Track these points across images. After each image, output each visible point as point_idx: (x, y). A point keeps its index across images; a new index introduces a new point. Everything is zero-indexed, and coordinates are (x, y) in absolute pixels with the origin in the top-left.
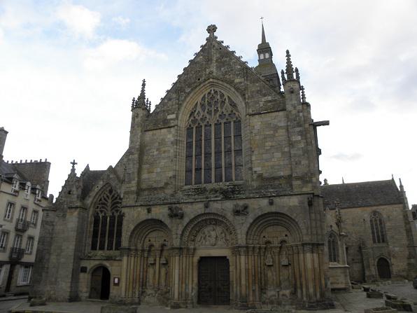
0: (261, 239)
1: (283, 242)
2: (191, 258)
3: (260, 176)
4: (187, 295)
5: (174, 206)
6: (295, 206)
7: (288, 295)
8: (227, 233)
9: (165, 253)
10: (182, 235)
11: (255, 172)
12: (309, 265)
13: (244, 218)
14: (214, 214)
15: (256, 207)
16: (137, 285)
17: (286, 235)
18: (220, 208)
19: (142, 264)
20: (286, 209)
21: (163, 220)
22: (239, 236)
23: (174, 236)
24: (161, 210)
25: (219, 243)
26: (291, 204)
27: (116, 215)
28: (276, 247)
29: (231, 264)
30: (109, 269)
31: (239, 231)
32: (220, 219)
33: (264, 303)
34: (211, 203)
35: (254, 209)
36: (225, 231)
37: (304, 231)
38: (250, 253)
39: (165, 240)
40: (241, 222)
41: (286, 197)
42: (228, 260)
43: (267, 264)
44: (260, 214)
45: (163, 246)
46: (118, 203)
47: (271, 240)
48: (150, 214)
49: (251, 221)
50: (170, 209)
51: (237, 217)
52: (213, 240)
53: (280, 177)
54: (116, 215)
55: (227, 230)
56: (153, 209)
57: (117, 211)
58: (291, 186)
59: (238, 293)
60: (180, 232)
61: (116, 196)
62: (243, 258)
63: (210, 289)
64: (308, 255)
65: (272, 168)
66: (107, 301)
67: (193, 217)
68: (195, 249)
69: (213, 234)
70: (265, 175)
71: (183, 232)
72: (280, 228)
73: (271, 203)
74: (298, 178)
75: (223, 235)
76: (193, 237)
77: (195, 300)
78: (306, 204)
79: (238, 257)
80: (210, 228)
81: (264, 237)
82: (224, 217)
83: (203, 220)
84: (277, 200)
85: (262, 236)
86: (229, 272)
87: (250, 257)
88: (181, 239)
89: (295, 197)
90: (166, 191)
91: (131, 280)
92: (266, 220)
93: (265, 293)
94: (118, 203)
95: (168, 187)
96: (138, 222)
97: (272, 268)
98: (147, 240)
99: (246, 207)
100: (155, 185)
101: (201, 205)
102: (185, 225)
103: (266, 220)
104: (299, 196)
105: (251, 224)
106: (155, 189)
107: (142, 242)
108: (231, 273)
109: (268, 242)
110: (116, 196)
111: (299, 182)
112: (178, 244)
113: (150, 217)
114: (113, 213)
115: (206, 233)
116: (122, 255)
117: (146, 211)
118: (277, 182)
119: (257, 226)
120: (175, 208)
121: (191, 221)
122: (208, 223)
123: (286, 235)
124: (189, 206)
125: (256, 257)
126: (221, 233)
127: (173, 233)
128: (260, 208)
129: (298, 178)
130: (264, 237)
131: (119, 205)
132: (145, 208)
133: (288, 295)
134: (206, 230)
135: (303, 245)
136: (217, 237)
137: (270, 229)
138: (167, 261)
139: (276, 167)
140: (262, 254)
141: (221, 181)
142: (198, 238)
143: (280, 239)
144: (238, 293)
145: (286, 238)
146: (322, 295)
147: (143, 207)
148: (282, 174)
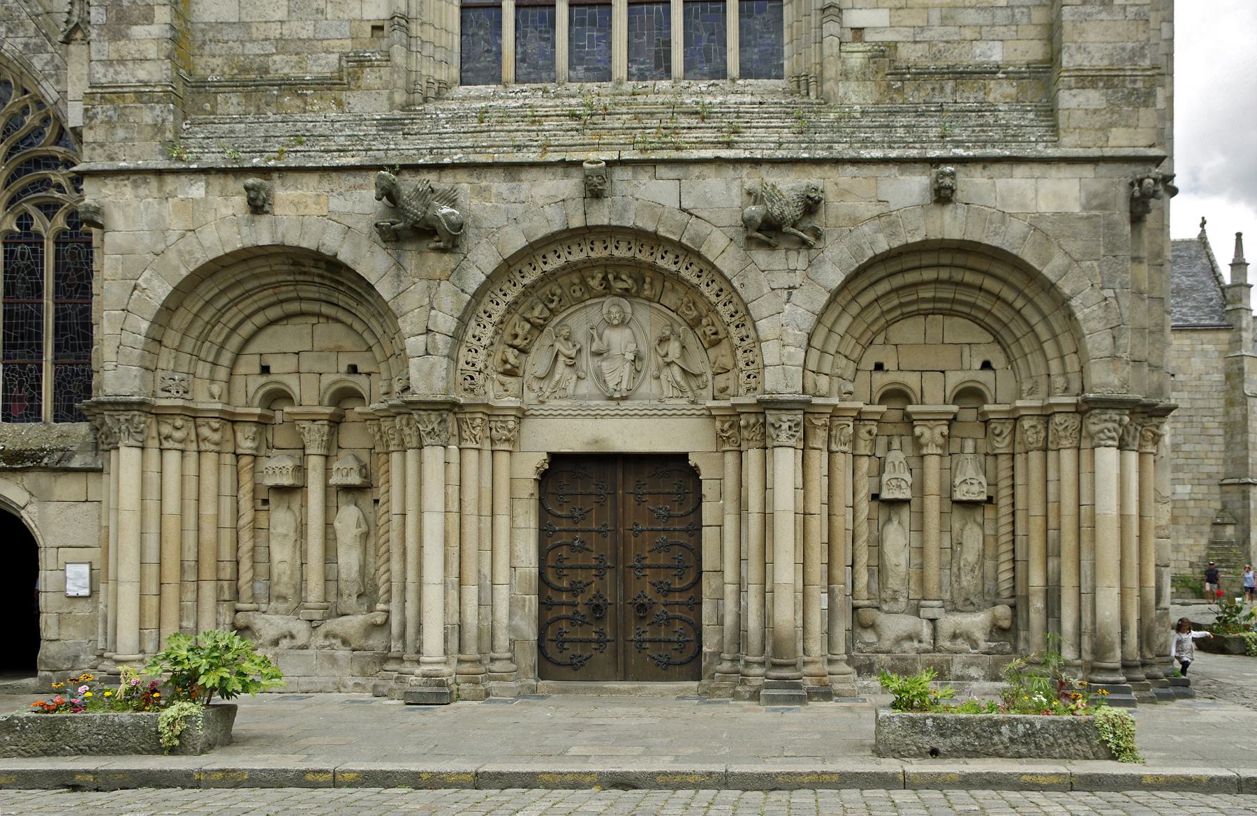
0: (863, 377)
1: (969, 394)
2: (503, 459)
3: (883, 54)
4: (488, 636)
5: (408, 184)
6: (1063, 218)
7: (980, 635)
8: (691, 339)
9: (352, 437)
10: (457, 338)
11: (858, 32)
12: (1108, 504)
13: (798, 260)
14: (638, 235)
15: (866, 209)
16: (208, 590)
17: (986, 365)
18: (672, 203)
19: (227, 488)
20: (1018, 227)
21: (344, 256)
22: (770, 352)
23: (415, 344)
24: (336, 203)
25: (648, 387)
26: (1045, 206)
27: (48, 228)
28: (931, 419)
29: (708, 488)
30: (29, 517)
31: (766, 327)
32: (667, 263)
33: (865, 669)
34: (620, 174)
35: (855, 221)
36: (682, 329)
37: (1097, 342)
38: (819, 439)
39: (353, 369)
40: (783, 280)
41: (1021, 170)
42: (694, 472)
43: (886, 495)
44: (883, 246)
45: (344, 396)
46: (50, 162)
47: (912, 380)
48: (264, 220)
49: (834, 277)
50: (389, 194)
51: (761, 256)
52: (618, 374)
53: (987, 72)
54: (48, 228)
55: (694, 324)
56: (284, 194)
57: (49, 209)
58: (1050, 112)
59: (753, 622)
60: (445, 322)
61: (30, 120)
62: (786, 462)
63: (597, 609)
64: (1108, 457)
65: (944, 21)
66: (30, 682)
67: (520, 242)
68: (522, 415)
69: (618, 339)
70: (909, 54)
71: (463, 322)
72: (959, 330)
73: (943, 196)
74: (1086, 80)
75: (674, 348)
76: (511, 355)
77: (529, 658)
78: (1121, 214)
79: (753, 457)
80: (611, 307)
81: (879, 367)
82: (689, 253)
83: (569, 268)
84: (972, 183)
85: (868, 363)
86: (696, 529)
87: (814, 455)
88: (452, 358)
89: (1067, 171)
90: (358, 102)
91: (172, 573)
92: (898, 281)
93: (872, 626)
94: (50, 162)
95: (369, 77)
96: (201, 258)
97: (905, 513)
98: (249, 365)
99: (811, 205)
100: (282, 66)
101: (569, 186)
102: (473, 286)
103: (898, 281)
104: (1087, 171)
105: (835, 296)
106: (291, 86)
107: (222, 373)
108: (709, 535)
109: (897, 395)
110: (30, 120)
111: (1094, 98)
112: (439, 385)
113: (262, 234)
114: (24, 221)
115: (580, 335)
116: (103, 444)
117: (240, 201)
118: (969, 97)
119: (854, 309)
120: (421, 195)
121: (509, 266)
122: (594, 283)
123: (986, 365)
124: (497, 184)
125: (840, 460)
126: (663, 340)
127: (405, 326)
128: (886, 219)
129: (1086, 80)
130: (879, 367)
131: (59, 176)
132: (236, 186)
133: (980, 635)
134: (579, 322)
135: (1085, 408)
136: (637, 357)
137: (909, 331)
138: (364, 470)
139: (971, 17)
140: (863, 448)
141: (668, 74)
142: (537, 362)
143: (955, 379)
144: (753, 622)
145: (986, 376)
146: (1146, 637)
147: (217, 182)
148: (996, 54)
